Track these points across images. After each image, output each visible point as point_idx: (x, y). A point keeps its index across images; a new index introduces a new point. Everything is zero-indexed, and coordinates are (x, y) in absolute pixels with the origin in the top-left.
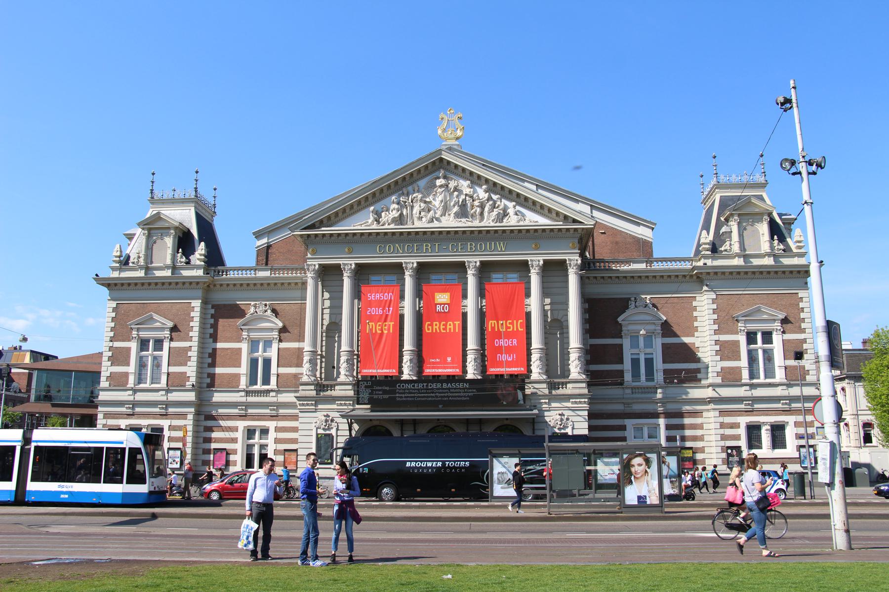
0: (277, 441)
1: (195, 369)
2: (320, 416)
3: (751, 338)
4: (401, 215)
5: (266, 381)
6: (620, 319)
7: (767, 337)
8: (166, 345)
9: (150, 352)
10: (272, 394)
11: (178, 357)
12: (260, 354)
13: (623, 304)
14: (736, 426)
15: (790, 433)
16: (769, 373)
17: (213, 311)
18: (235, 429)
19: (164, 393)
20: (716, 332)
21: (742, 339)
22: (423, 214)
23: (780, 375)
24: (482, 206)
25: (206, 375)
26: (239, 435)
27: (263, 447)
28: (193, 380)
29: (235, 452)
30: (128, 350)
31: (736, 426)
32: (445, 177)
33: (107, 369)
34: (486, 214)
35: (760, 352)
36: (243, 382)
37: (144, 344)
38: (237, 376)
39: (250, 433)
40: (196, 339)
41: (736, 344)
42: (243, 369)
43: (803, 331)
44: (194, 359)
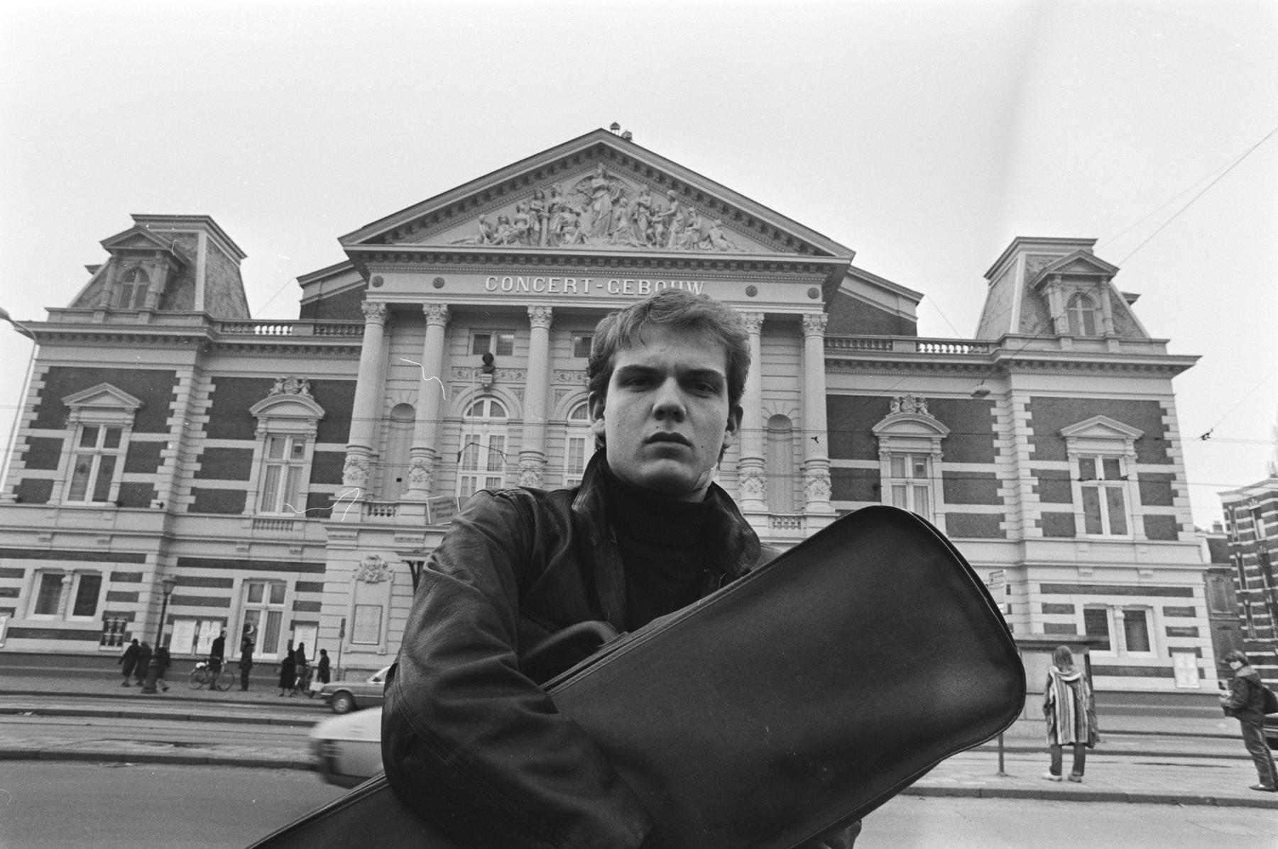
1: (169, 478)
2: (362, 556)
3: (1087, 466)
4: (529, 230)
6: (876, 429)
7: (1112, 466)
9: (97, 449)
10: (297, 526)
11: (144, 458)
14: (1070, 609)
15: (1156, 624)
16: (1119, 527)
17: (212, 388)
18: (228, 583)
19: (108, 515)
20: (1033, 457)
21: (1074, 469)
22: (566, 229)
23: (1136, 529)
24: (667, 223)
25: (188, 491)
28: (163, 496)
31: (1070, 609)
32: (605, 176)
34: (673, 234)
35: (1102, 494)
37: (89, 435)
38: (242, 494)
43: (1170, 461)
44: (170, 463)
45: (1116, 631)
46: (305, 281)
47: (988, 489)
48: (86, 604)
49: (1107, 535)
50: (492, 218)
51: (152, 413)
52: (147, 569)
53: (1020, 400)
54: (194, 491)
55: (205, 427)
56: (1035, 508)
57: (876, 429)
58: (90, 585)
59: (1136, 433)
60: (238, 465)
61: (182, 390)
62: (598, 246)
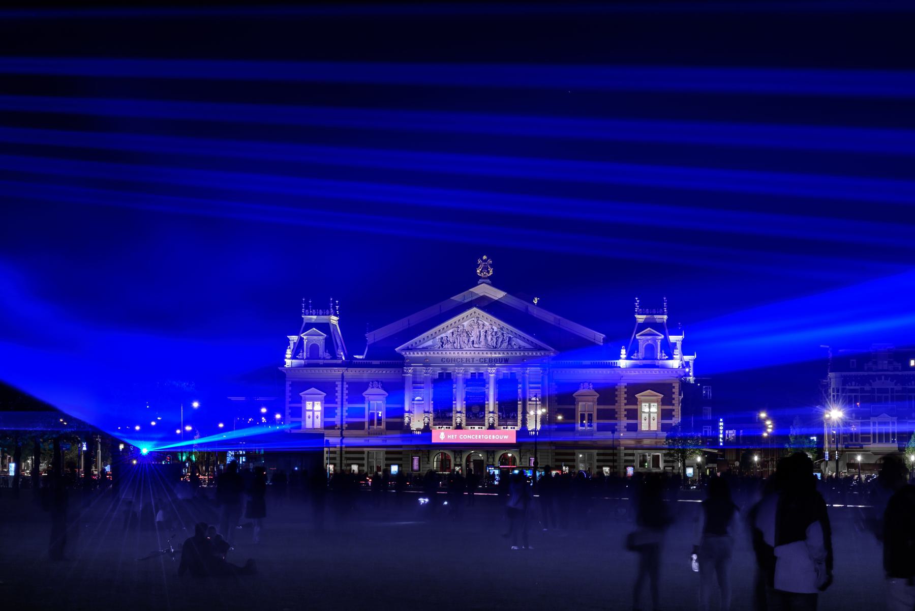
13: (576, 386)
20: (626, 404)
28: (339, 426)
29: (363, 465)
40: (339, 403)
47: (612, 415)
54: (347, 423)
55: (347, 400)
56: (624, 422)
61: (339, 389)
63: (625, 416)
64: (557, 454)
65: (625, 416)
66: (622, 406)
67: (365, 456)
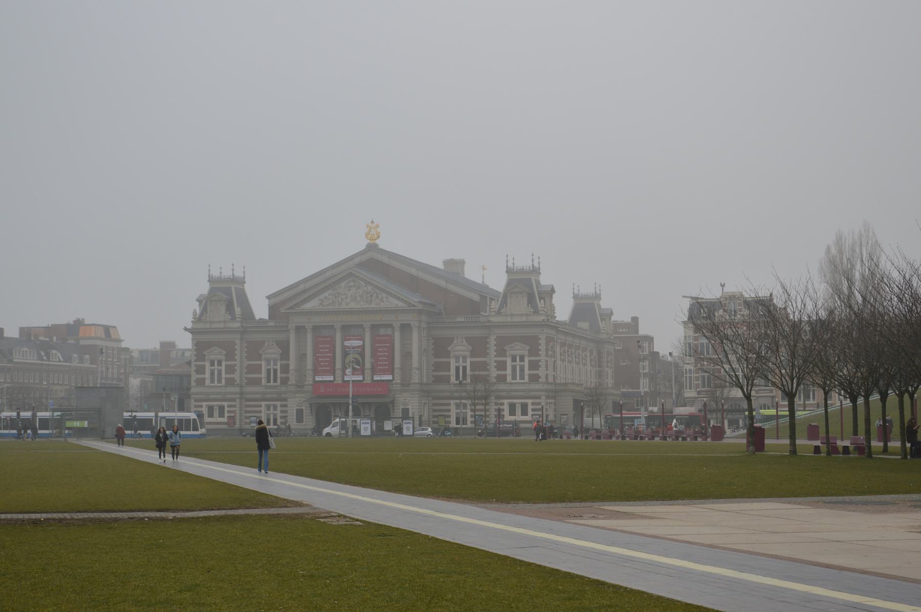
0: (281, 412)
3: (514, 359)
5: (275, 381)
6: (449, 349)
7: (522, 359)
8: (224, 364)
12: (272, 366)
13: (450, 340)
15: (530, 407)
16: (522, 377)
20: (495, 356)
21: (509, 360)
23: (527, 378)
24: (371, 296)
26: (263, 409)
27: (275, 415)
28: (238, 381)
30: (204, 366)
33: (194, 377)
36: (264, 382)
38: (260, 379)
39: (268, 407)
41: (505, 362)
42: (264, 375)
45: (518, 410)
46: (268, 297)
47: (484, 366)
48: (221, 414)
49: (518, 380)
50: (322, 297)
51: (230, 356)
52: (237, 403)
53: (493, 337)
57: (449, 349)
58: (222, 409)
59: (528, 348)
60: (258, 369)
61: (238, 347)
62: (353, 305)
63: (495, 367)
64: (434, 405)
65: (495, 367)
66: (492, 359)
67: (263, 409)
